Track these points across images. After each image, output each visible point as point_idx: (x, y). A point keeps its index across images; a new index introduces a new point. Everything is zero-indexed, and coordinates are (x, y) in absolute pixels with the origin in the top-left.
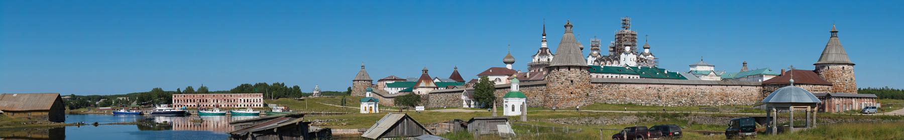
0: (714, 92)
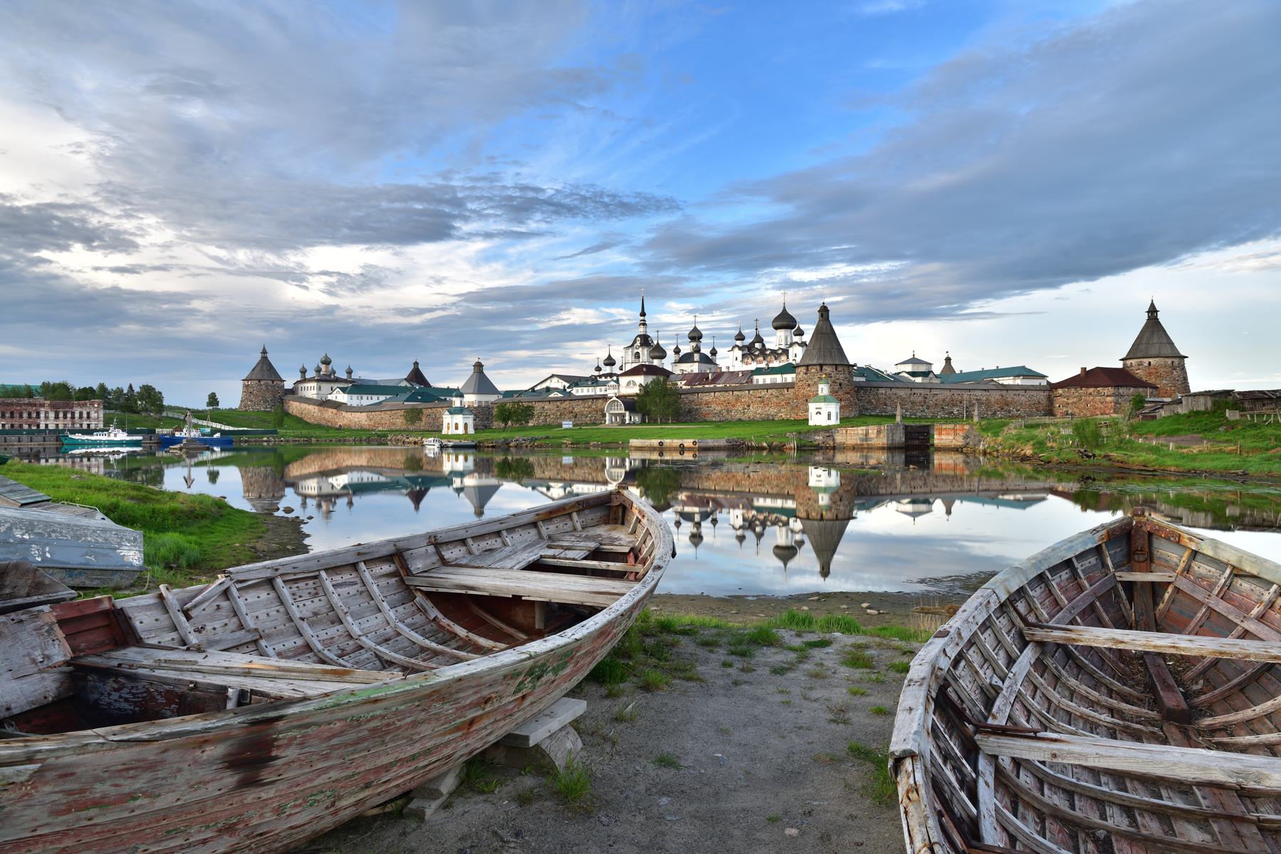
0: (992, 399)
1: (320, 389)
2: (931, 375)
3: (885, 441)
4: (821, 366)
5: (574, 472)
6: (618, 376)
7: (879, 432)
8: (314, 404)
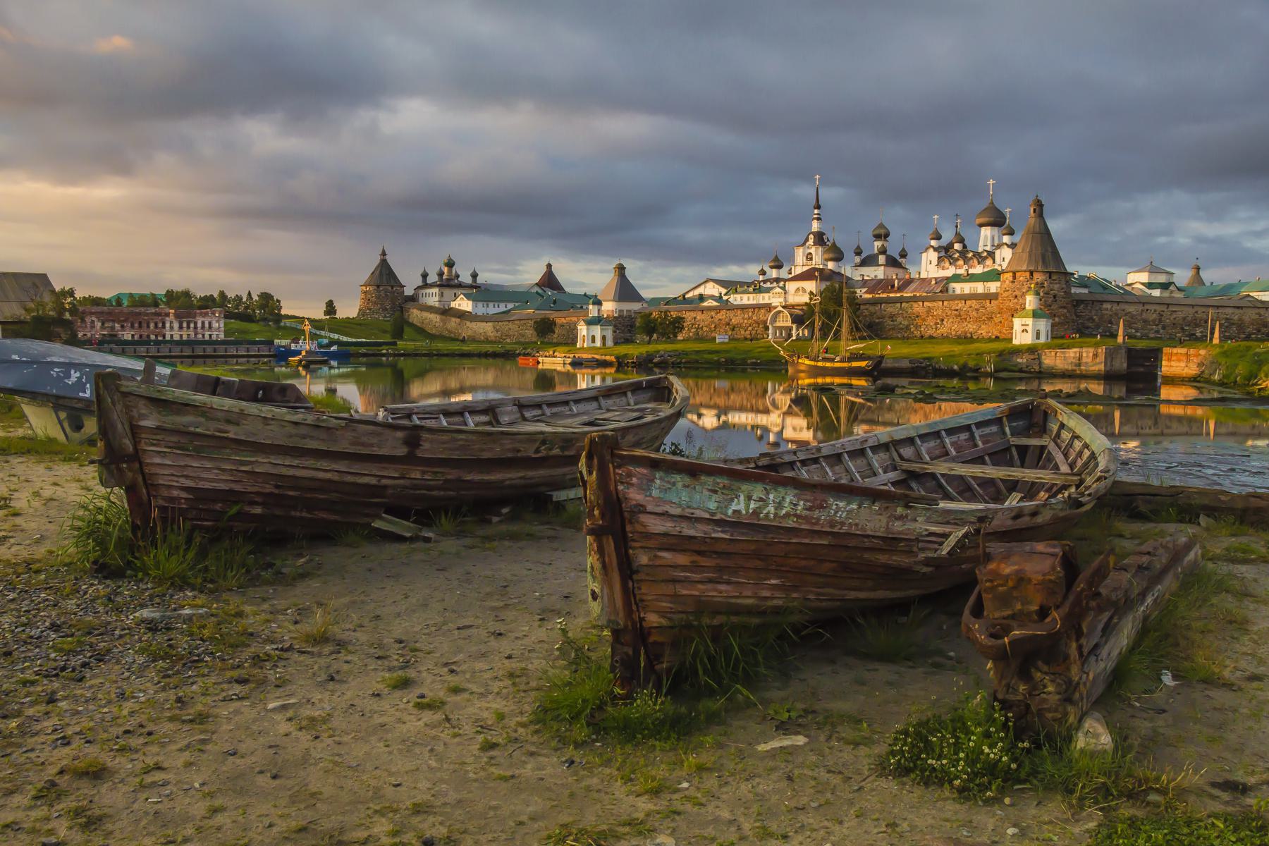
0: (1246, 319)
1: (442, 295)
2: (1172, 288)
3: (1102, 367)
4: (1032, 274)
5: (729, 398)
6: (785, 281)
7: (1095, 355)
8: (436, 313)
